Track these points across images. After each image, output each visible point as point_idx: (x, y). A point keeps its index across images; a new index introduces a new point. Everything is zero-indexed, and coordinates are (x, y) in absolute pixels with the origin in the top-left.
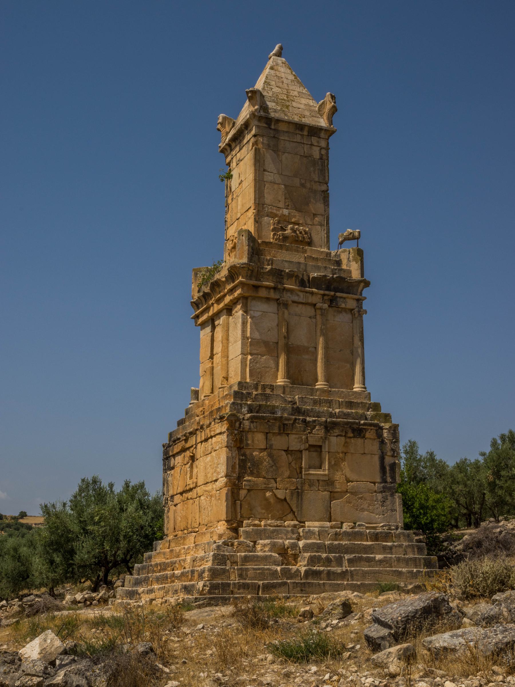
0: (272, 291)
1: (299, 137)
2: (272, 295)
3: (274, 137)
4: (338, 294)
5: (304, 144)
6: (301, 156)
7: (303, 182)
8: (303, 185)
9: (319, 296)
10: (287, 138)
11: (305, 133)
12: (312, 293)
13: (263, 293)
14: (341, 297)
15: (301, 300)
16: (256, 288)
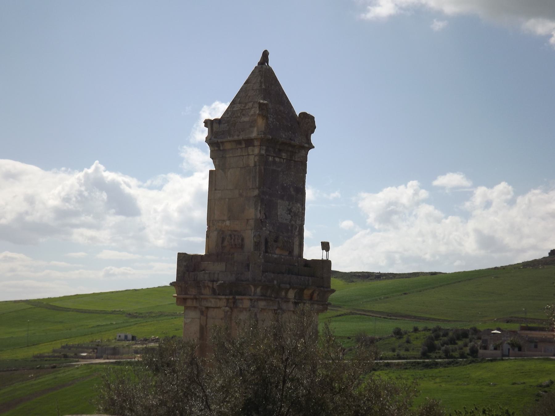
0: (195, 301)
1: (239, 150)
2: (195, 304)
3: (223, 157)
4: (237, 297)
5: (243, 156)
6: (241, 168)
7: (241, 191)
8: (241, 195)
9: (225, 300)
10: (231, 155)
11: (244, 146)
12: (219, 299)
13: (189, 303)
14: (239, 299)
15: (212, 306)
16: (185, 300)
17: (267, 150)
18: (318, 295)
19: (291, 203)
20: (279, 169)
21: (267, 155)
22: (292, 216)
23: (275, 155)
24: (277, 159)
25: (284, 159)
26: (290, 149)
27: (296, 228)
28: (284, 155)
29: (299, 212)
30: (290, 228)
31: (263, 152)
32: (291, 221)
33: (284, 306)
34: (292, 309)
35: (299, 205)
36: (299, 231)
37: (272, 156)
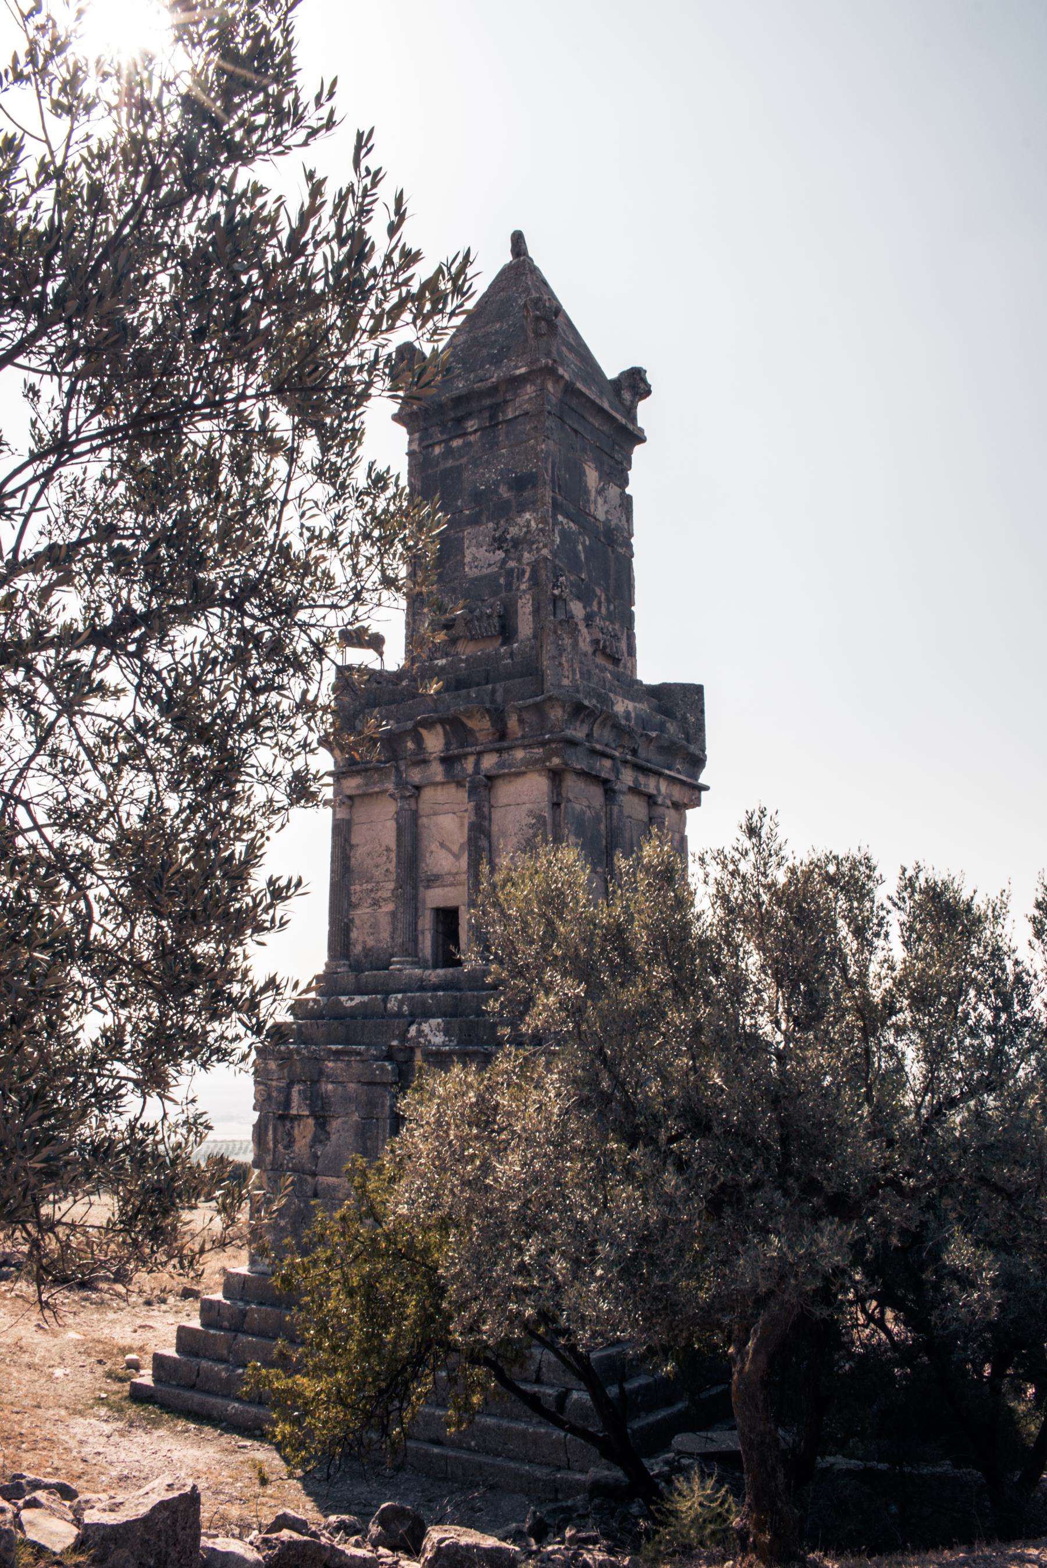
17: (421, 440)
18: (521, 721)
19: (502, 522)
20: (464, 461)
21: (428, 447)
22: (506, 551)
23: (445, 437)
24: (456, 443)
25: (475, 431)
26: (487, 402)
27: (524, 572)
28: (471, 425)
29: (526, 533)
30: (502, 581)
31: (415, 447)
32: (504, 562)
33: (415, 775)
34: (439, 778)
35: (527, 516)
36: (529, 579)
37: (439, 443)
